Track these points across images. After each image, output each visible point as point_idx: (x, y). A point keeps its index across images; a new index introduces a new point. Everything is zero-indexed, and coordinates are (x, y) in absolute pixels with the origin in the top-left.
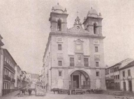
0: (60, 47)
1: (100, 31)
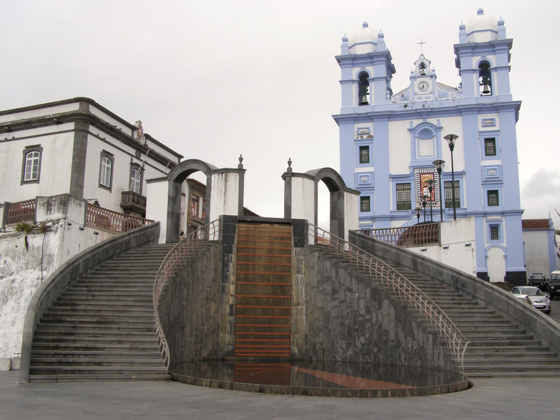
0: (364, 152)
1: (506, 85)
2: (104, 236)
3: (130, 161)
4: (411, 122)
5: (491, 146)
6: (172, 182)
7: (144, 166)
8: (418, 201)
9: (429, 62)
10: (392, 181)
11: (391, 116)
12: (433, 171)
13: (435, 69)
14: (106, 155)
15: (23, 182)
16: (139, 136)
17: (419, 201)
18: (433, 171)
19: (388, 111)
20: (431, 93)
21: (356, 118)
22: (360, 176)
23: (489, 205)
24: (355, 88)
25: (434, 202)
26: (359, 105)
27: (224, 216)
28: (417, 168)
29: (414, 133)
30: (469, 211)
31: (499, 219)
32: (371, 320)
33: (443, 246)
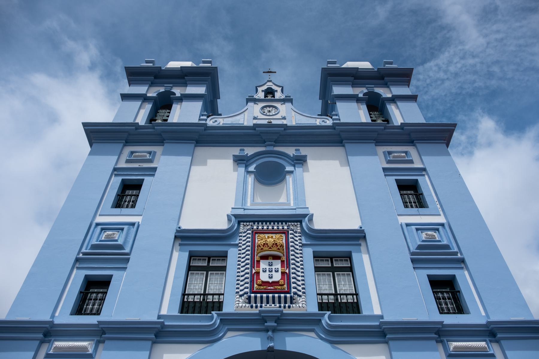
8: (241, 293)
10: (180, 245)
12: (286, 227)
17: (246, 290)
18: (286, 227)
25: (288, 295)
28: (247, 222)
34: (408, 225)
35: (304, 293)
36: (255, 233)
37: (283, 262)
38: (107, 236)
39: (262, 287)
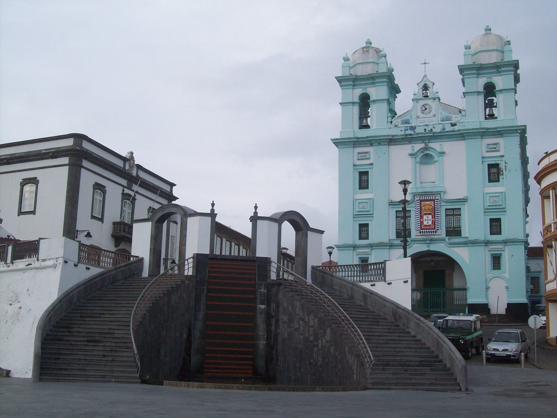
0: (364, 178)
2: (95, 271)
3: (121, 192)
4: (413, 147)
5: (495, 171)
6: (154, 223)
7: (135, 196)
9: (432, 83)
11: (392, 141)
12: (434, 198)
13: (438, 91)
14: (98, 187)
15: (20, 213)
16: (131, 167)
18: (434, 198)
19: (388, 136)
20: (434, 116)
21: (356, 142)
22: (359, 203)
23: (492, 233)
24: (356, 110)
25: (434, 230)
26: (360, 128)
27: (198, 255)
29: (415, 158)
30: (470, 239)
31: (501, 248)
32: (317, 346)
33: (387, 282)
34: (487, 194)
35: (440, 229)
36: (421, 201)
37: (432, 216)
38: (362, 207)
39: (424, 227)
